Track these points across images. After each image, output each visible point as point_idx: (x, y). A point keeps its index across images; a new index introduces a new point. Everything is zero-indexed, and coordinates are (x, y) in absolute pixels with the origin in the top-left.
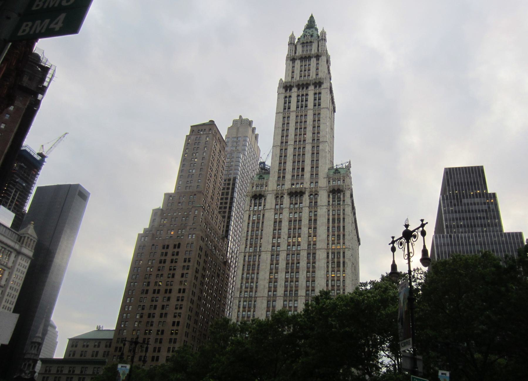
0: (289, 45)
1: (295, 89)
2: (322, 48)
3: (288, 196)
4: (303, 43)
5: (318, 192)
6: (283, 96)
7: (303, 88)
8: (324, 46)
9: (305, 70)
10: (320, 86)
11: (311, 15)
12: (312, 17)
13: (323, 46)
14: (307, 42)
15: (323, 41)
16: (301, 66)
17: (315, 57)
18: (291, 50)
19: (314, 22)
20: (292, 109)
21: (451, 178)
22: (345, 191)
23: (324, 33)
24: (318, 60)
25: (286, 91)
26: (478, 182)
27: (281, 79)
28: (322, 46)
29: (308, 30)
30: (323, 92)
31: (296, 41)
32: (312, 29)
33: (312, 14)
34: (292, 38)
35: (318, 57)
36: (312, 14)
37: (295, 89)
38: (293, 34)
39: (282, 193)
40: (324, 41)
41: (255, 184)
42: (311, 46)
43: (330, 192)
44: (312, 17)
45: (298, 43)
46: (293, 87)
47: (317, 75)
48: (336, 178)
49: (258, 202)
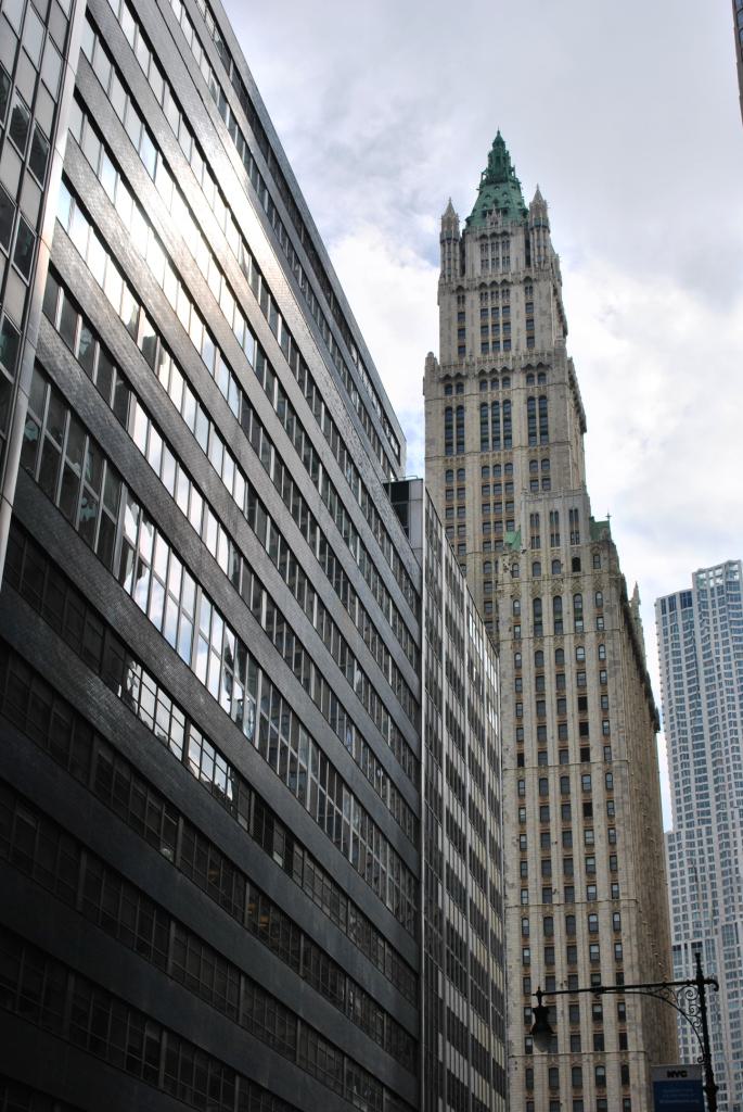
0: (442, 242)
1: (471, 387)
2: (539, 255)
4: (484, 237)
6: (441, 408)
8: (545, 247)
9: (495, 332)
10: (542, 376)
11: (496, 135)
12: (499, 143)
13: (542, 248)
14: (494, 235)
15: (541, 232)
16: (484, 311)
18: (449, 260)
19: (506, 158)
20: (468, 447)
23: (540, 206)
25: (448, 390)
28: (539, 247)
29: (490, 189)
30: (552, 395)
31: (462, 226)
32: (503, 187)
33: (499, 133)
34: (449, 220)
36: (499, 133)
38: (450, 208)
40: (544, 232)
42: (506, 245)
44: (499, 143)
45: (468, 237)
47: (531, 339)
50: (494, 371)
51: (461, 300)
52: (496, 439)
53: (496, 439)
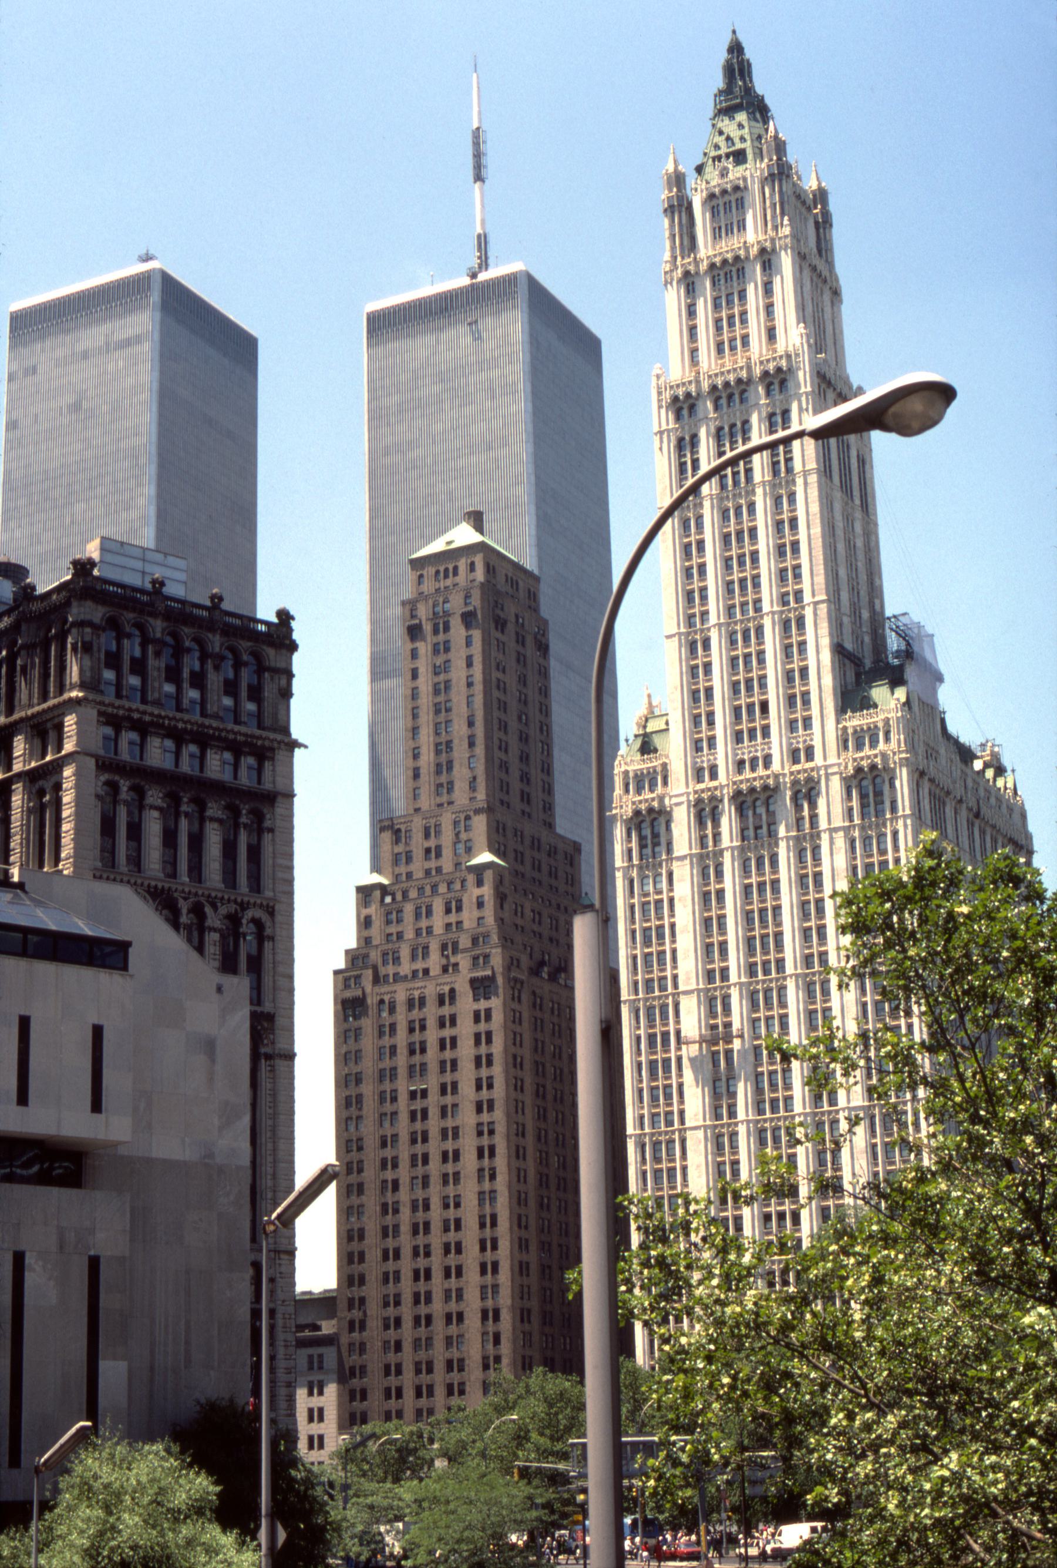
12: (736, 48)
39: (713, 798)
44: (736, 48)
49: (647, 832)
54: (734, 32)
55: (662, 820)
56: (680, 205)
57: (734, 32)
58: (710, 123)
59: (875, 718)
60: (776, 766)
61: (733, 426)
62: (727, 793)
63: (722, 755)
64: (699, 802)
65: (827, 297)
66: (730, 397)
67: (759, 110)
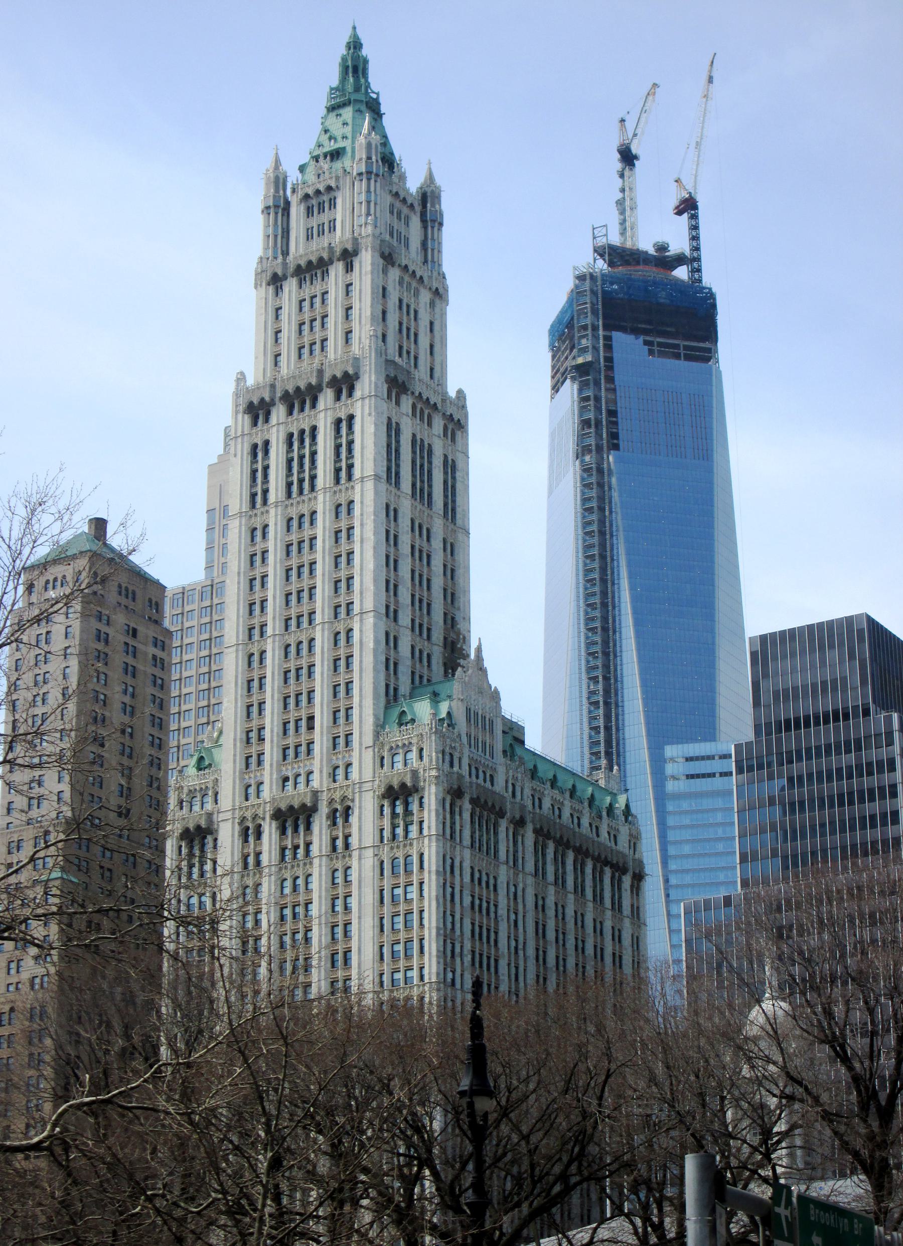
1: (279, 413)
3: (274, 824)
5: (353, 801)
7: (302, 410)
11: (349, 32)
12: (355, 45)
14: (318, 192)
17: (339, 260)
21: (766, 675)
22: (423, 789)
24: (349, 268)
26: (843, 679)
27: (241, 378)
35: (348, 257)
37: (279, 413)
39: (255, 817)
41: (186, 790)
42: (333, 203)
43: (384, 797)
44: (355, 45)
46: (272, 403)
48: (400, 744)
50: (298, 389)
51: (278, 290)
52: (301, 481)
53: (301, 481)
54: (354, 28)
55: (209, 839)
56: (276, 206)
57: (354, 28)
58: (320, 121)
59: (410, 734)
60: (315, 784)
61: (302, 432)
62: (269, 810)
63: (269, 775)
64: (243, 819)
65: (425, 296)
66: (303, 403)
67: (374, 108)
